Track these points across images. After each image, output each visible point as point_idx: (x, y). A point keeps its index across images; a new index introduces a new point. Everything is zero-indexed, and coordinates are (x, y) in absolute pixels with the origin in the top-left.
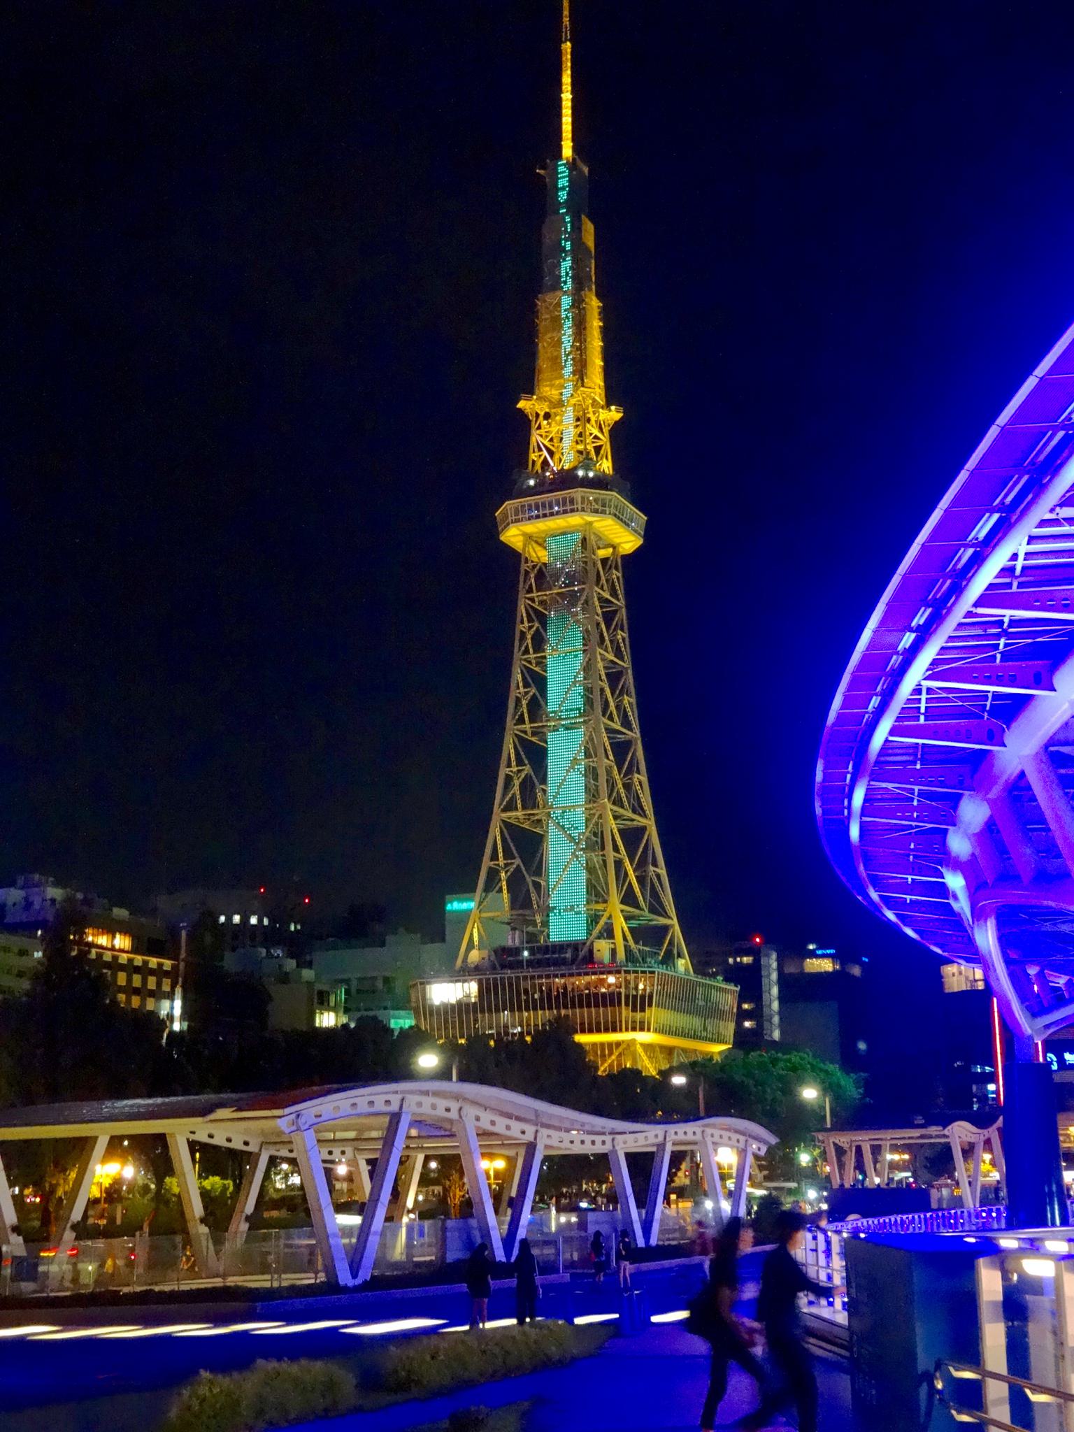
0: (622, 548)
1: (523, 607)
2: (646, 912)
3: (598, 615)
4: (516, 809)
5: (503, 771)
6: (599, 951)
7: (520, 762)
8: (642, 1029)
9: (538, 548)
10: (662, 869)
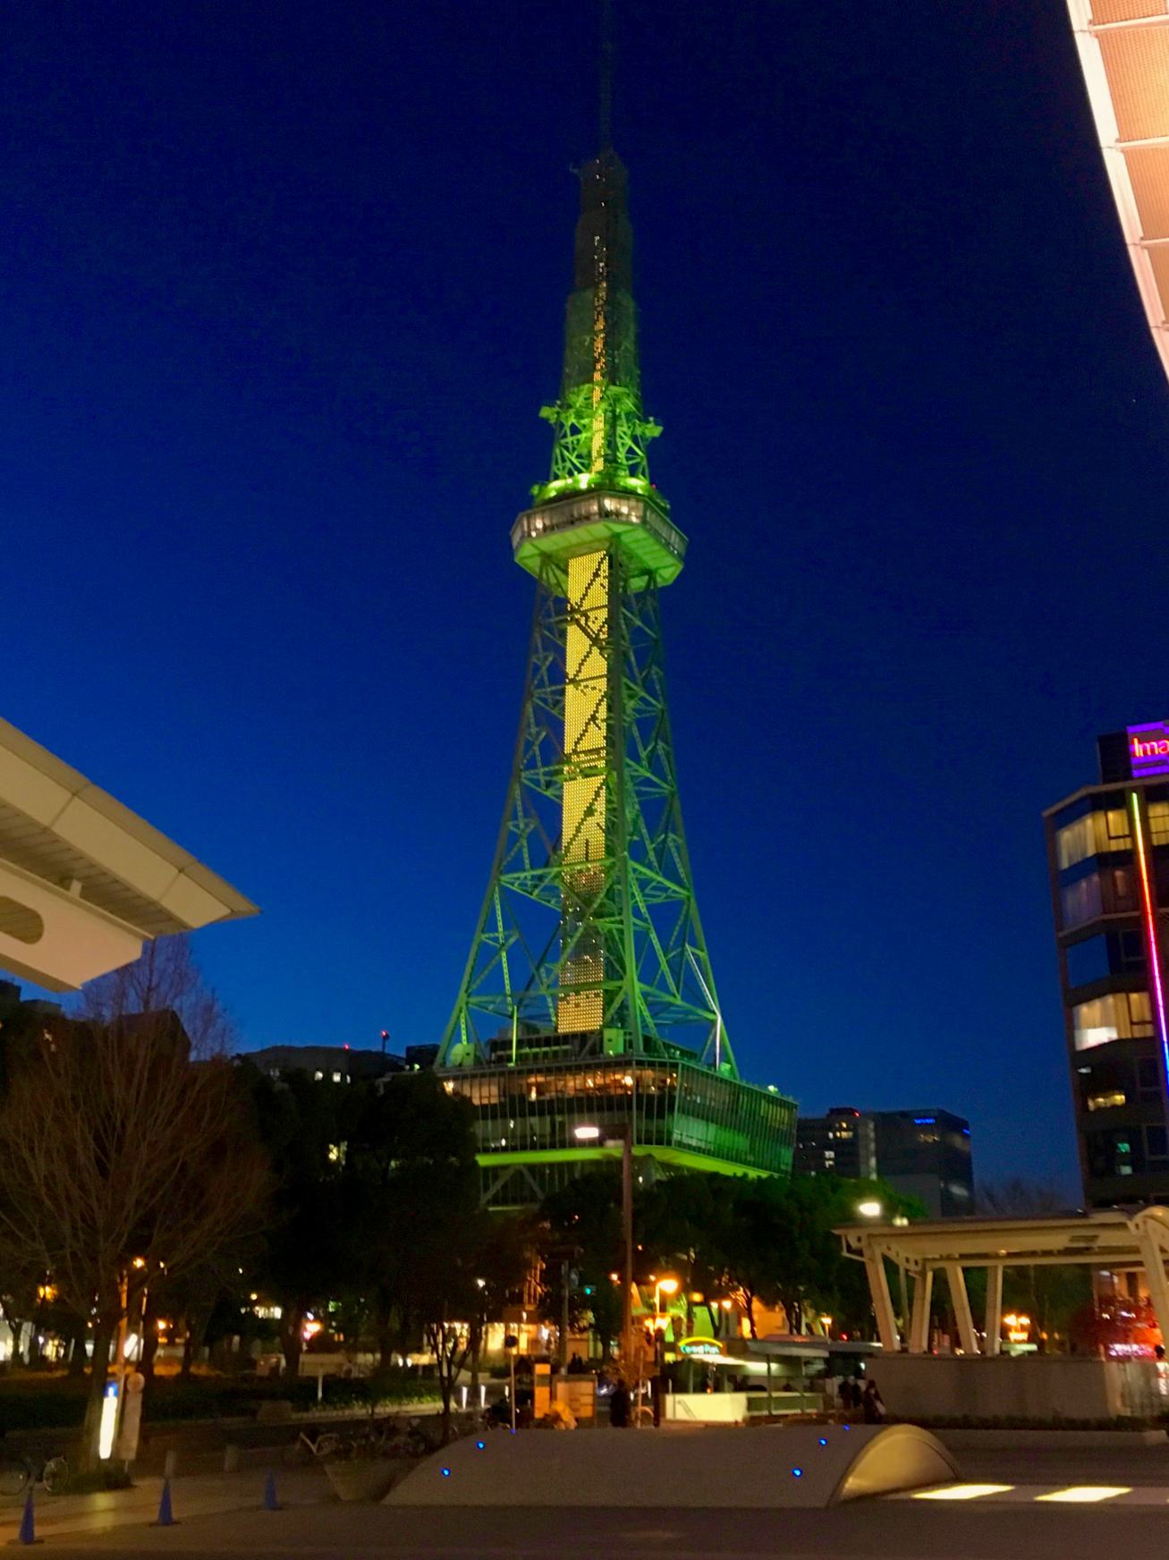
0: (661, 576)
2: (678, 1001)
6: (610, 1040)
7: (526, 813)
8: (659, 1142)
9: (558, 572)
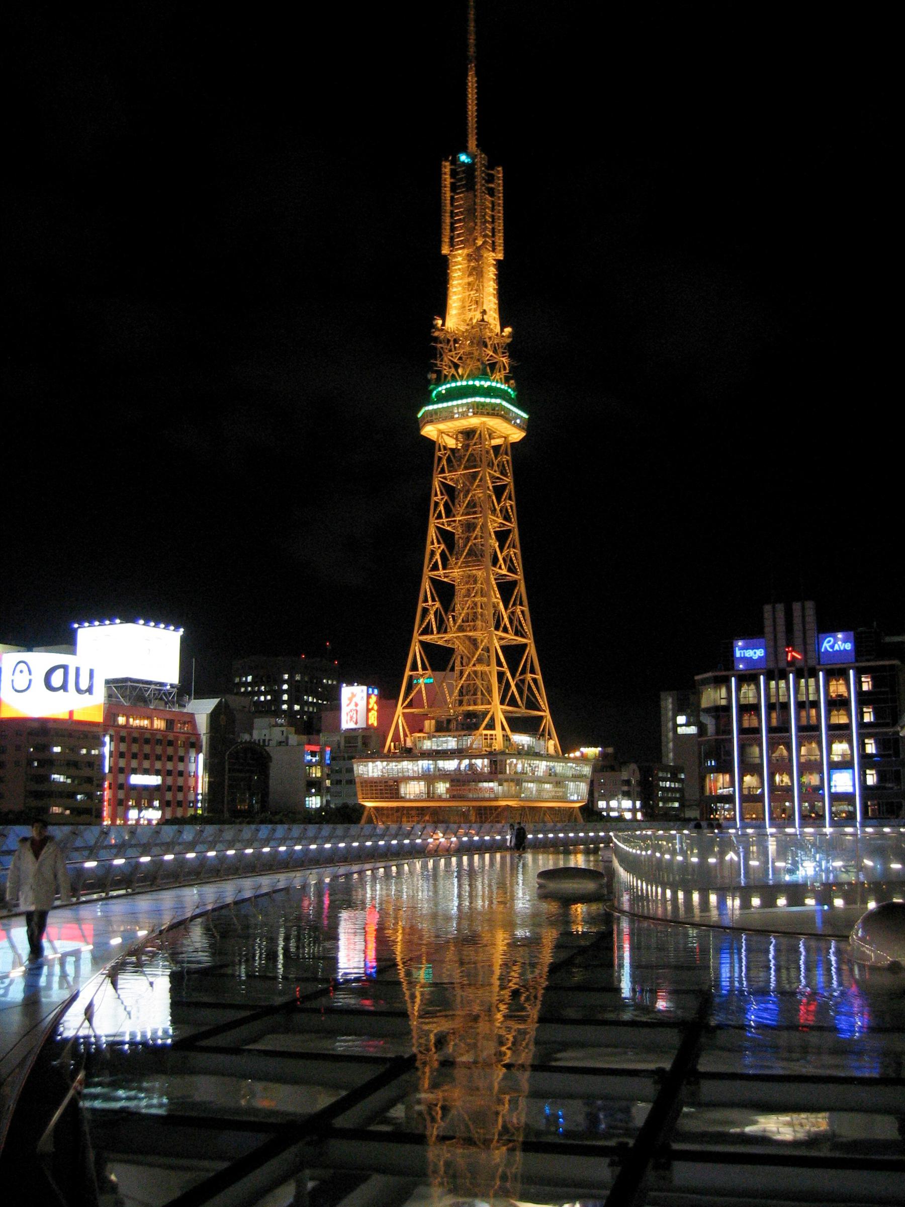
1: (436, 483)
3: (490, 490)
4: (432, 633)
5: (421, 605)
10: (538, 675)
